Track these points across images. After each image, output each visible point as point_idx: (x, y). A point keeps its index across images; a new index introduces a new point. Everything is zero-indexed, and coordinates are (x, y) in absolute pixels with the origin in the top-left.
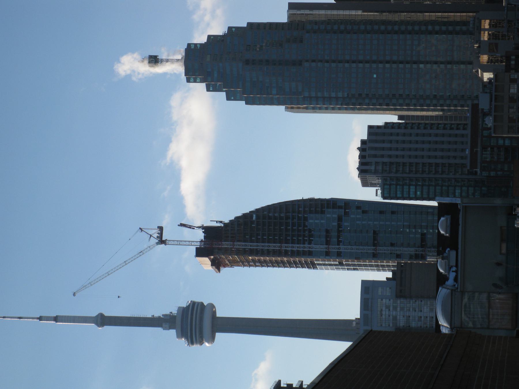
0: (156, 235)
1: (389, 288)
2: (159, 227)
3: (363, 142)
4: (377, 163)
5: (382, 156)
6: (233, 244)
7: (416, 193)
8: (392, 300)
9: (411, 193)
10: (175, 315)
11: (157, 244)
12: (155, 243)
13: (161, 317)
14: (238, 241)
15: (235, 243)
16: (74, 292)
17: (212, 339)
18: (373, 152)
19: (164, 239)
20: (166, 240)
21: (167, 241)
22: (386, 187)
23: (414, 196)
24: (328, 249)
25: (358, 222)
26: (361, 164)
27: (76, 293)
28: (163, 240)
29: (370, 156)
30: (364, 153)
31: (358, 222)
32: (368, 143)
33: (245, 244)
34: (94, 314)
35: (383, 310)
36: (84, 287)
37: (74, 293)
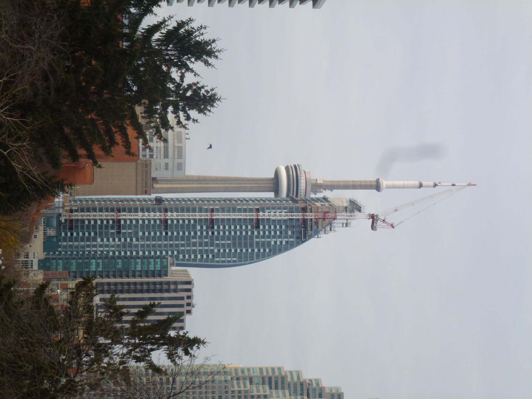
1: (158, 169)
2: (376, 230)
3: (189, 312)
4: (175, 291)
6: (304, 217)
7: (136, 263)
8: (155, 157)
9: (140, 263)
10: (312, 193)
11: (377, 216)
13: (324, 191)
14: (298, 220)
15: (302, 217)
17: (277, 174)
19: (371, 220)
20: (369, 219)
21: (368, 217)
22: (166, 269)
23: (137, 260)
24: (211, 215)
25: (183, 242)
26: (189, 290)
28: (372, 219)
29: (182, 298)
30: (189, 301)
31: (183, 242)
32: (185, 313)
33: (292, 216)
34: (384, 192)
35: (163, 148)
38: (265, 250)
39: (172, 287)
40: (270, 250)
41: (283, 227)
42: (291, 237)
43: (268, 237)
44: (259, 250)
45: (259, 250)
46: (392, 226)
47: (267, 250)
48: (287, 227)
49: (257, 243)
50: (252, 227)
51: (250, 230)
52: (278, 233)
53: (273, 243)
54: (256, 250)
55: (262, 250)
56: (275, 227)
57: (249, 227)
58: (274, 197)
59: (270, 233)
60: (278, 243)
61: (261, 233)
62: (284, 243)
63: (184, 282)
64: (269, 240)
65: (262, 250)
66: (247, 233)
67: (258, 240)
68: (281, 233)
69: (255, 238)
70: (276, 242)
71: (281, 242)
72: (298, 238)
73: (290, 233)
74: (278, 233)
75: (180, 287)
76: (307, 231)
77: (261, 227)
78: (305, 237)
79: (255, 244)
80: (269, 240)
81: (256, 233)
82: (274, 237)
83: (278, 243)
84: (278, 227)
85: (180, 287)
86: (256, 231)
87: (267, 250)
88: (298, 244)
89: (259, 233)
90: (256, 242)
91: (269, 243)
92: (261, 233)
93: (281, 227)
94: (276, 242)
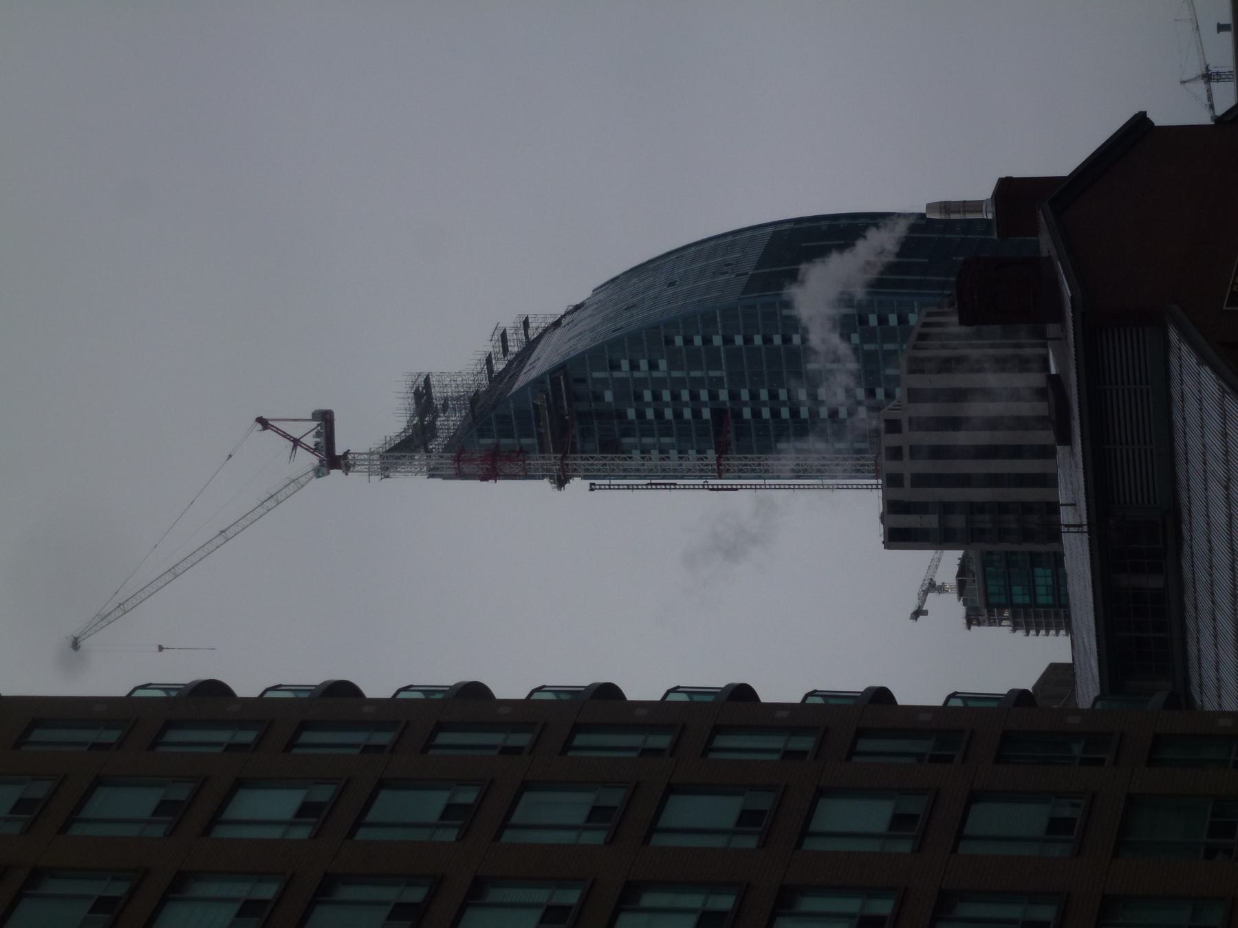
0: (310, 441)
4: (946, 508)
5: (964, 480)
11: (319, 472)
12: (310, 468)
16: (76, 636)
18: (925, 466)
19: (339, 451)
20: (347, 453)
21: (350, 457)
22: (989, 569)
27: (83, 637)
36: (104, 619)
37: (76, 639)
38: (688, 341)
39: (958, 521)
40: (669, 341)
41: (631, 414)
42: (604, 382)
43: (681, 381)
44: (707, 341)
45: (707, 341)
46: (264, 423)
47: (679, 341)
48: (622, 415)
49: (714, 363)
50: (738, 415)
51: (745, 404)
52: (647, 395)
53: (663, 364)
54: (717, 340)
55: (698, 341)
56: (659, 415)
57: (747, 413)
58: (701, 344)
59: (676, 397)
60: (644, 364)
61: (704, 395)
62: (625, 365)
63: (916, 540)
64: (676, 374)
65: (698, 341)
66: (754, 396)
67: (713, 373)
68: (639, 397)
69: (725, 379)
70: (653, 366)
71: (634, 366)
72: (582, 381)
73: (609, 396)
74: (647, 395)
75: (931, 521)
76: (551, 398)
77: (706, 414)
78: (555, 382)
79: (723, 361)
80: (676, 374)
81: (723, 395)
82: (661, 382)
83: (644, 364)
84: (650, 414)
85: (931, 521)
86: (724, 403)
87: (679, 341)
88: (579, 359)
89: (713, 396)
90: (720, 369)
91: (672, 366)
92: (704, 395)
93: (641, 415)
94: (653, 366)
